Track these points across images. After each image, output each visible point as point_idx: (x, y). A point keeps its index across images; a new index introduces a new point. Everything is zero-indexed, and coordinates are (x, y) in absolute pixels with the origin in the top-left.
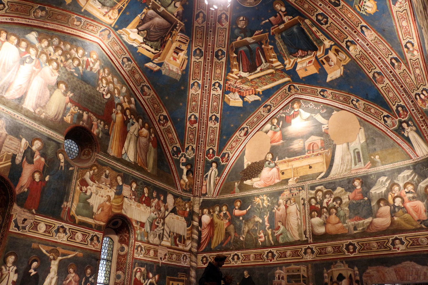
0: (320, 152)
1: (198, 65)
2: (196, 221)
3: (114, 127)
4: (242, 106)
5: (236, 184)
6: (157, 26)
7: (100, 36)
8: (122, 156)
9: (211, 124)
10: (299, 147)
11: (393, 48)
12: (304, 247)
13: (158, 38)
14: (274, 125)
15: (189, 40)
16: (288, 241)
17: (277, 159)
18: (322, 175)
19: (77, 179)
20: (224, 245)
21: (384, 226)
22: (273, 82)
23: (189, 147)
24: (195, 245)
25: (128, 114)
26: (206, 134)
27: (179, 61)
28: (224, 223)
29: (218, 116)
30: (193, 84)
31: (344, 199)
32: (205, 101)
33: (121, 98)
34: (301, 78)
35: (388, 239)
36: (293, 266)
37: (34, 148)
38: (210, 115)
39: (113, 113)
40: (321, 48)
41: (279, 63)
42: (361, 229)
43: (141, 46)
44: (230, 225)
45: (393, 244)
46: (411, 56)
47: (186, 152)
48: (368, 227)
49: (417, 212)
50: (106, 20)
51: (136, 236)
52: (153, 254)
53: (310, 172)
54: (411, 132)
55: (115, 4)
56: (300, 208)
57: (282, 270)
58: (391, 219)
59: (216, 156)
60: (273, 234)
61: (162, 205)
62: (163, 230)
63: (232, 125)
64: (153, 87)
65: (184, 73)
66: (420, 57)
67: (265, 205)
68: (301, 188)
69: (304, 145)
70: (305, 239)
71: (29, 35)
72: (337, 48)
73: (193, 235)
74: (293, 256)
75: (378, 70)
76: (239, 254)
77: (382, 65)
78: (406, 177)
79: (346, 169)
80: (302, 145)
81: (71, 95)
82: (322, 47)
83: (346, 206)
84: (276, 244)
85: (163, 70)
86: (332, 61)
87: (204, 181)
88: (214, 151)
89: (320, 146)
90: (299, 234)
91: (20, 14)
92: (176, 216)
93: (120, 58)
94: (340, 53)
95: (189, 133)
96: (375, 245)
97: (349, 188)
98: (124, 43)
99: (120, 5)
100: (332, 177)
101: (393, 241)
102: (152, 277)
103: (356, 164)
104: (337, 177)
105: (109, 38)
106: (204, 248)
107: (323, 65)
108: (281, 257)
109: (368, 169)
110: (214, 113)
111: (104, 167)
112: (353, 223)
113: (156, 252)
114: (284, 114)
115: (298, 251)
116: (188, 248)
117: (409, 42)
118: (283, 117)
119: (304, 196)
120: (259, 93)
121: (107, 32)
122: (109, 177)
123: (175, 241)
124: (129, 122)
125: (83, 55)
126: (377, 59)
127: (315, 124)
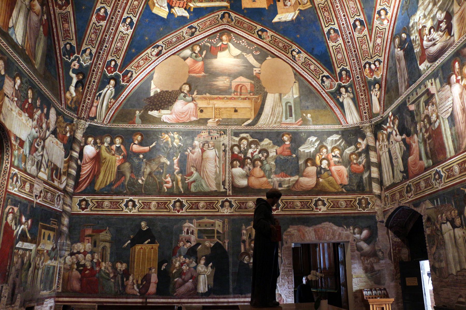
0: (249, 96)
2: (76, 152)
4: (166, 17)
5: (138, 112)
9: (122, 28)
10: (224, 85)
11: (364, 10)
12: (221, 199)
14: (195, 53)
16: (202, 190)
17: (195, 93)
18: (249, 121)
20: (114, 187)
21: (310, 186)
23: (86, 49)
24: (72, 182)
26: (113, 38)
28: (116, 160)
29: (135, 20)
31: (271, 152)
34: (243, 7)
35: (311, 199)
36: (206, 220)
38: (125, 15)
42: (286, 186)
44: (125, 162)
45: (316, 205)
46: (380, 24)
47: (82, 55)
48: (294, 185)
49: (340, 176)
51: (13, 160)
52: (29, 188)
53: (235, 116)
54: (347, 98)
56: (220, 154)
57: (192, 223)
58: (317, 180)
59: (117, 72)
60: (183, 180)
61: (44, 120)
62: (42, 156)
63: (147, 38)
66: (387, 28)
67: (175, 144)
68: (222, 132)
69: (231, 85)
70: (224, 190)
73: (70, 170)
74: (206, 209)
75: (336, 27)
76: (136, 200)
77: (344, 23)
78: (334, 143)
79: (276, 120)
80: (229, 83)
83: (273, 160)
84: (186, 193)
87: (95, 101)
88: (116, 65)
89: (249, 90)
90: (216, 184)
92: (56, 140)
95: (92, 31)
96: (299, 204)
97: (278, 142)
100: (260, 126)
101: (317, 201)
102: (25, 222)
103: (286, 118)
104: (266, 127)
106: (83, 188)
107: (277, 2)
108: (191, 208)
109: (299, 125)
112: (279, 179)
113: (32, 186)
114: (209, 43)
115: (214, 203)
116: (62, 187)
117: (384, 9)
118: (208, 46)
119: (226, 142)
120: (190, 8)
123: (52, 176)
126: (342, 15)
127: (245, 65)
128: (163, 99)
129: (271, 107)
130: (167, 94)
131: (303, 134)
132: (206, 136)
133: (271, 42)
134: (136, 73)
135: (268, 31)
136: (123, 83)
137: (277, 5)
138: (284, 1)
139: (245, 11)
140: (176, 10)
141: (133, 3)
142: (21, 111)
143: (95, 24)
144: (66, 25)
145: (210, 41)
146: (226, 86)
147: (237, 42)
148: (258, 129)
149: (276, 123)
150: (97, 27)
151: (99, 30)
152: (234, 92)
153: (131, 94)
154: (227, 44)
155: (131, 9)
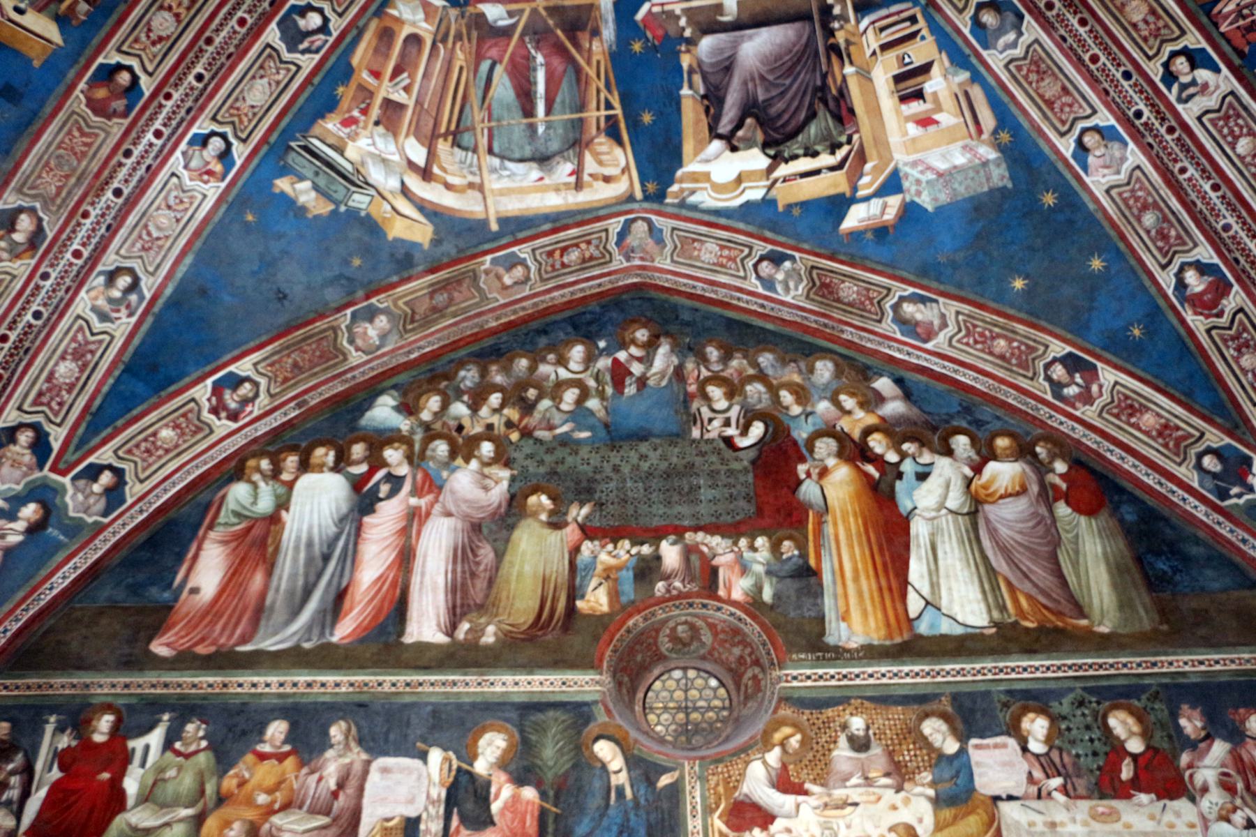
1: (1036, 65)
3: (829, 529)
6: (772, 71)
7: (628, 259)
8: (911, 628)
13: (807, 99)
15: (917, 11)
19: (708, 811)
25: (878, 450)
27: (947, 118)
30: (1081, 148)
32: (1183, 170)
33: (823, 406)
37: (481, 767)
39: (799, 483)
43: (775, 181)
50: (599, 193)
55: (580, 124)
64: (934, 285)
65: (1005, 137)
71: (368, 414)
81: (585, 510)
85: (919, 193)
91: (315, 374)
93: (745, 278)
95: (1230, 353)
98: (715, 219)
99: (594, 115)
105: (660, 242)
111: (830, 712)
121: (640, 227)
122: (874, 743)
124: (900, 476)
125: (589, 359)
141: (1239, 156)
142: (1105, 802)
143: (1215, 327)
144: (1148, 420)
150: (1230, 328)
151: (1245, 330)
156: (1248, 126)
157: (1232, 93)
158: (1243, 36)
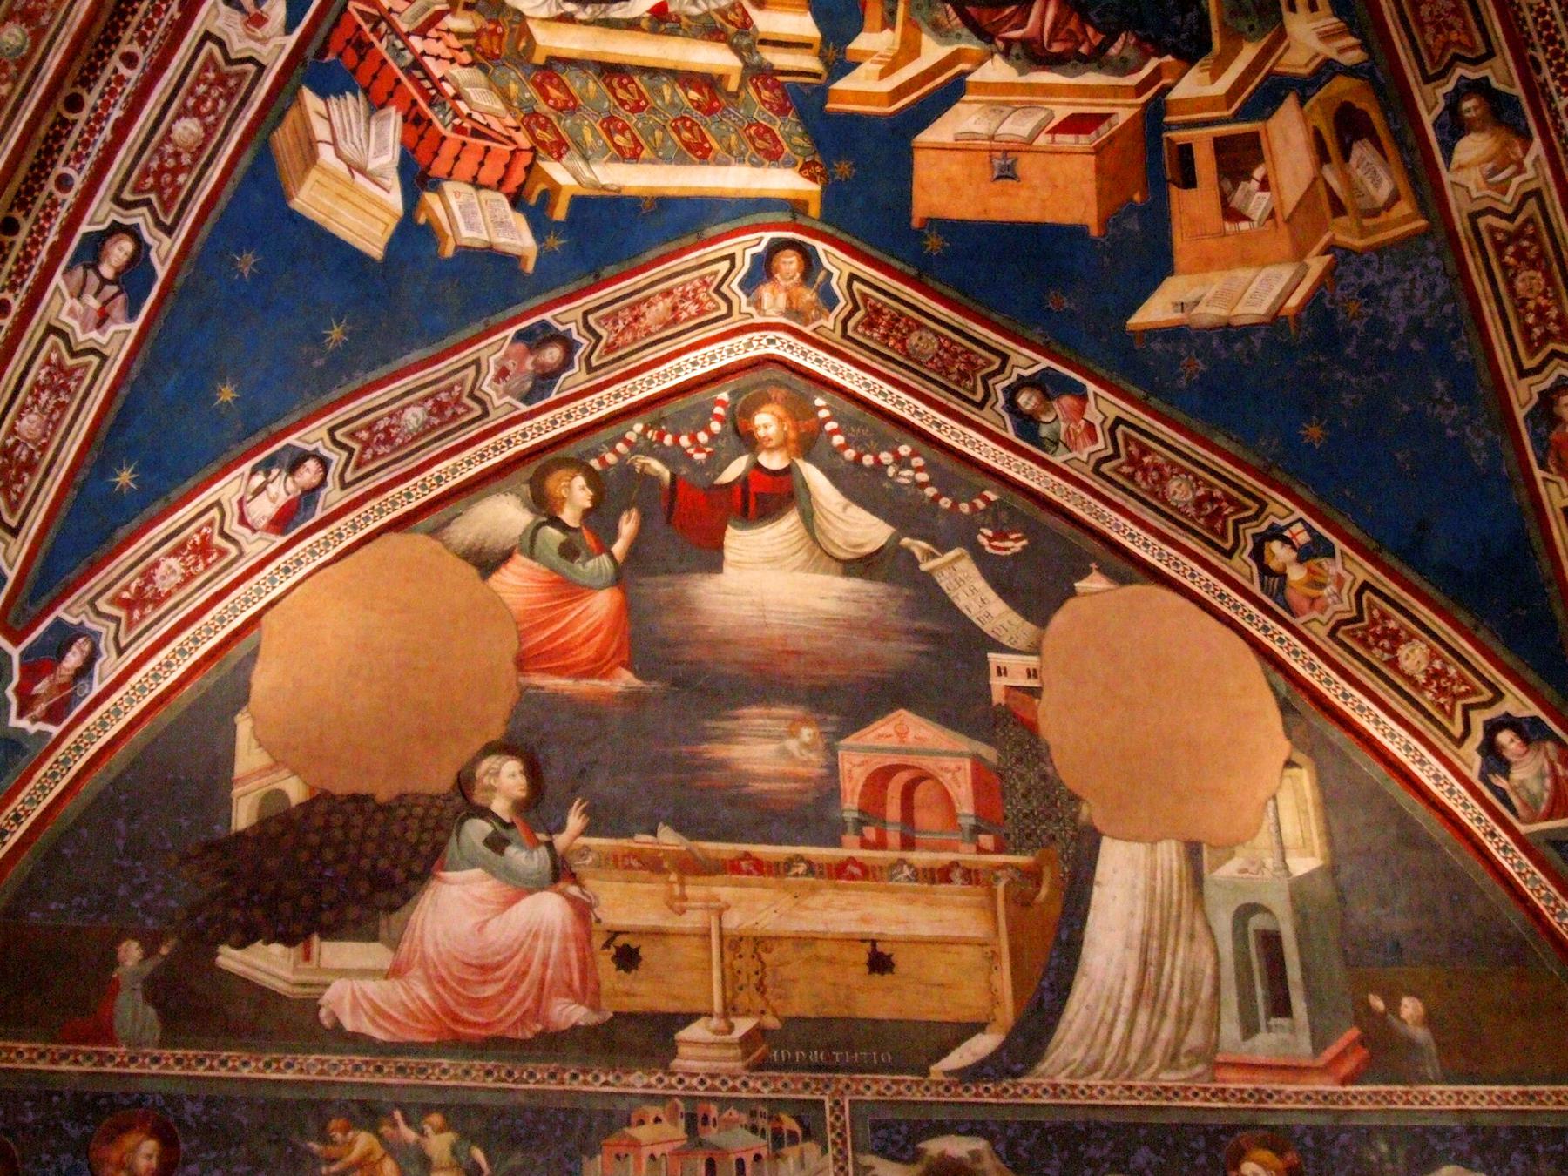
0: (967, 855)
4: (376, 251)
5: (131, 952)
10: (785, 767)
14: (555, 521)
17: (575, 821)
18: (983, 1045)
22: (681, 160)
29: (164, 251)
32: (130, 60)
38: (101, 214)
40: (1236, 53)
41: (802, 25)
68: (789, 1124)
69: (833, 768)
72: (1366, 104)
79: (1179, 1040)
82: (1249, 53)
86: (1264, 185)
89: (966, 807)
94: (1362, 152)
100: (1062, 1079)
103: (1250, 1029)
104: (1100, 1089)
107: (1174, 190)
109: (1344, 1082)
110: (140, 218)
114: (664, 460)
118: (650, 480)
120: (551, 192)
128: (329, 855)
129: (1136, 943)
130: (358, 820)
131: (1384, 1148)
132: (667, 1148)
133: (1105, 468)
134: (121, 651)
135: (1091, 388)
136: (24, 723)
137: (1174, 208)
138: (1228, 185)
139: (934, 243)
140: (454, 203)
141: (169, 131)
145: (668, 440)
146: (796, 778)
147: (858, 459)
148: (1046, 1100)
149: (1174, 1057)
152: (860, 823)
153: (71, 808)
154: (787, 471)
155: (146, 173)
156: (218, 120)
157: (261, 68)
158: (348, 42)
